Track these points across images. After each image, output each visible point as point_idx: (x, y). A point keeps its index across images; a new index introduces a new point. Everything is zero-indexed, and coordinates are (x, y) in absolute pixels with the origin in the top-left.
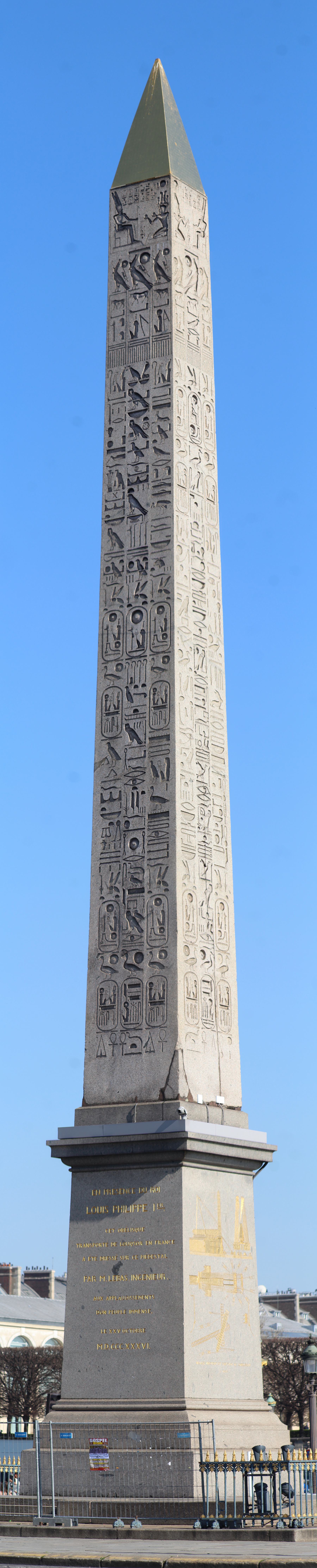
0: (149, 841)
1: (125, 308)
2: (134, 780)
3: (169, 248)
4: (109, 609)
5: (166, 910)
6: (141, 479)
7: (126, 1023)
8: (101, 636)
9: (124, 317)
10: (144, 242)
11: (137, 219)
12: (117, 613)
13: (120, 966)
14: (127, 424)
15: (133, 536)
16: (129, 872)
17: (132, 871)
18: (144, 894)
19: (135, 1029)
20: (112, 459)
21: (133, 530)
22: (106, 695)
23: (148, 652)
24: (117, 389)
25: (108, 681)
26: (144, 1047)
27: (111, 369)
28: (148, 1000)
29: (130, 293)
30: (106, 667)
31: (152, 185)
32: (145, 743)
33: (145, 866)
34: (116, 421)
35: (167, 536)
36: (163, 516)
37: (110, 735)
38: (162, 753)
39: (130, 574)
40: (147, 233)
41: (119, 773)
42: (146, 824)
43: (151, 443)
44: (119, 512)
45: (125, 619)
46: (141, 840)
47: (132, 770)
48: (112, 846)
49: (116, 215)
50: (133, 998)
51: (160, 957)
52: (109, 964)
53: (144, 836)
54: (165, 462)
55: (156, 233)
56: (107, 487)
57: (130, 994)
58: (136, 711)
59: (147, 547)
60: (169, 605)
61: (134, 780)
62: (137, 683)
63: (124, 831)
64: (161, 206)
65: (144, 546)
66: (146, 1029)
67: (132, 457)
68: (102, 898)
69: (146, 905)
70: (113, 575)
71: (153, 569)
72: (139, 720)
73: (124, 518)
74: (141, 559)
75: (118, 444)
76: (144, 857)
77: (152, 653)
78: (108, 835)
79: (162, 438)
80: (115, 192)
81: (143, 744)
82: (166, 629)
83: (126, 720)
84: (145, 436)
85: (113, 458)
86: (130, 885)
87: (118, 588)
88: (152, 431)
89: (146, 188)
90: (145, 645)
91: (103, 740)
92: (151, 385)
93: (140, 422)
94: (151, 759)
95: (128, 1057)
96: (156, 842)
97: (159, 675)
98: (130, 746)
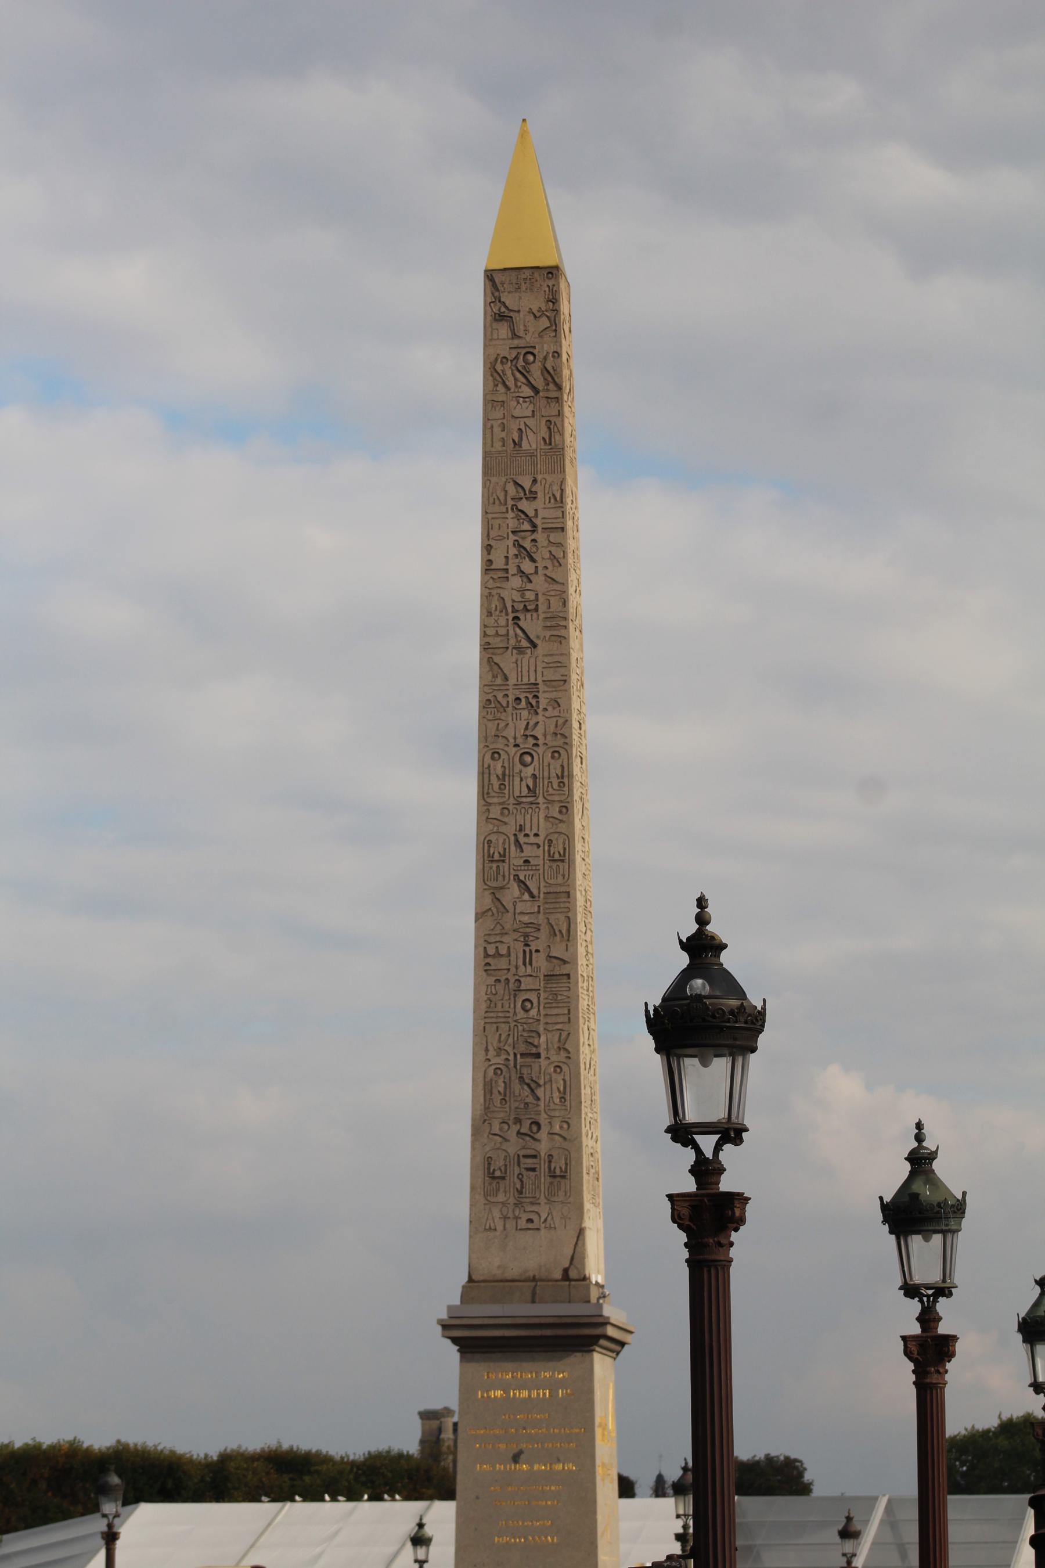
0: (546, 1003)
1: (505, 412)
2: (526, 935)
3: (559, 351)
4: (491, 747)
5: (567, 1078)
6: (529, 608)
7: (521, 1196)
8: (481, 776)
9: (505, 421)
10: (528, 340)
11: (519, 311)
12: (501, 752)
13: (512, 1134)
14: (510, 543)
15: (519, 670)
16: (521, 1035)
17: (525, 1034)
18: (540, 1060)
19: (532, 1203)
20: (491, 581)
21: (519, 663)
22: (488, 841)
23: (541, 800)
24: (497, 502)
25: (491, 827)
26: (543, 1223)
27: (489, 478)
28: (547, 1174)
29: (511, 395)
30: (488, 810)
31: (536, 275)
32: (539, 897)
33: (541, 1029)
34: (497, 538)
35: (562, 675)
36: (556, 652)
37: (494, 884)
38: (560, 910)
39: (516, 711)
40: (531, 330)
41: (508, 926)
42: (542, 985)
43: (540, 569)
44: (501, 641)
45: (511, 760)
46: (535, 1002)
47: (524, 926)
48: (499, 1005)
49: (493, 302)
50: (528, 1169)
51: (561, 1127)
52: (498, 1132)
53: (539, 998)
54: (558, 593)
55: (542, 331)
56: (485, 610)
57: (525, 1166)
58: (526, 861)
59: (537, 684)
60: (566, 751)
61: (526, 935)
62: (527, 831)
63: (514, 990)
64: (548, 301)
65: (534, 682)
66: (545, 1203)
67: (516, 582)
68: (489, 1060)
69: (542, 1072)
70: (495, 709)
71: (545, 709)
72: (531, 873)
73: (507, 648)
74: (530, 696)
75: (499, 563)
76: (539, 1020)
77: (546, 801)
78: (494, 992)
79: (554, 566)
80: (491, 275)
81: (537, 899)
82: (563, 777)
83: (514, 870)
84: (533, 560)
85: (493, 579)
86: (522, 1048)
87: (502, 725)
88: (542, 555)
89: (529, 277)
90: (537, 792)
91: (485, 889)
92: (539, 504)
93: (527, 544)
94: (547, 916)
95: (522, 1232)
96: (554, 1005)
97: (555, 826)
98: (520, 900)
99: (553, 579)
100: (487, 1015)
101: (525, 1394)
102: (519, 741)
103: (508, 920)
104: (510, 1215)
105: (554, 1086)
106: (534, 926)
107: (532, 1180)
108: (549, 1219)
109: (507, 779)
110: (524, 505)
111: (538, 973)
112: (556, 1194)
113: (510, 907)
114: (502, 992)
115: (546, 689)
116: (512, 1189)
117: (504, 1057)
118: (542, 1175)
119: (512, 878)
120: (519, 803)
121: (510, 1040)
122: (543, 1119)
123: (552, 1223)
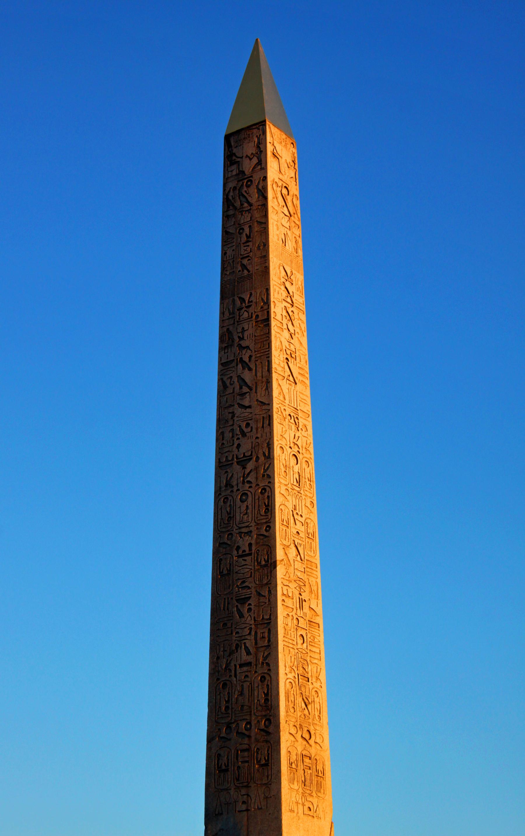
15: (290, 396)
21: (290, 390)
26: (315, 812)
33: (308, 659)
37: (284, 542)
40: (287, 174)
53: (307, 636)
62: (297, 511)
79: (301, 335)
94: (308, 576)
96: (313, 644)
99: (301, 343)
102: (292, 445)
104: (300, 801)
106: (303, 582)
108: (318, 809)
109: (287, 469)
110: (288, 284)
114: (290, 625)
115: (302, 416)
117: (293, 674)
119: (292, 540)
120: (293, 489)
121: (296, 663)
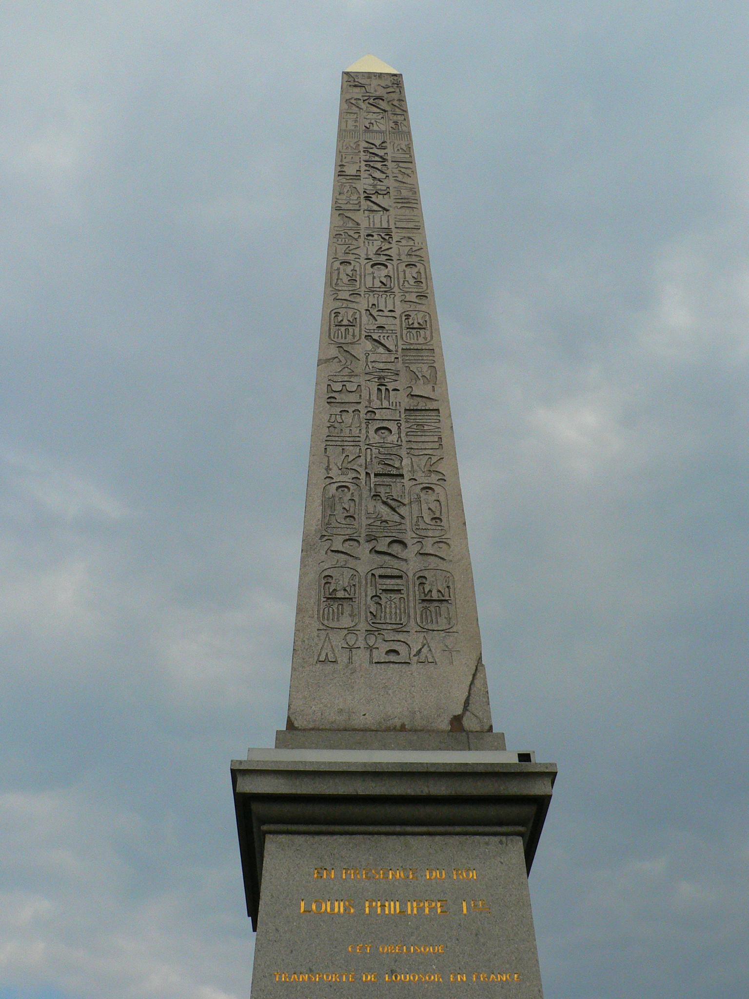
5: (442, 499)
26: (415, 656)
33: (403, 453)
47: (378, 370)
62: (382, 307)
72: (387, 335)
96: (419, 433)
100: (328, 438)
101: (393, 907)
103: (360, 367)
104: (361, 643)
105: (424, 507)
106: (392, 371)
107: (395, 603)
111: (398, 407)
112: (434, 621)
113: (362, 357)
116: (363, 613)
118: (411, 598)
122: (409, 537)
123: (429, 656)
